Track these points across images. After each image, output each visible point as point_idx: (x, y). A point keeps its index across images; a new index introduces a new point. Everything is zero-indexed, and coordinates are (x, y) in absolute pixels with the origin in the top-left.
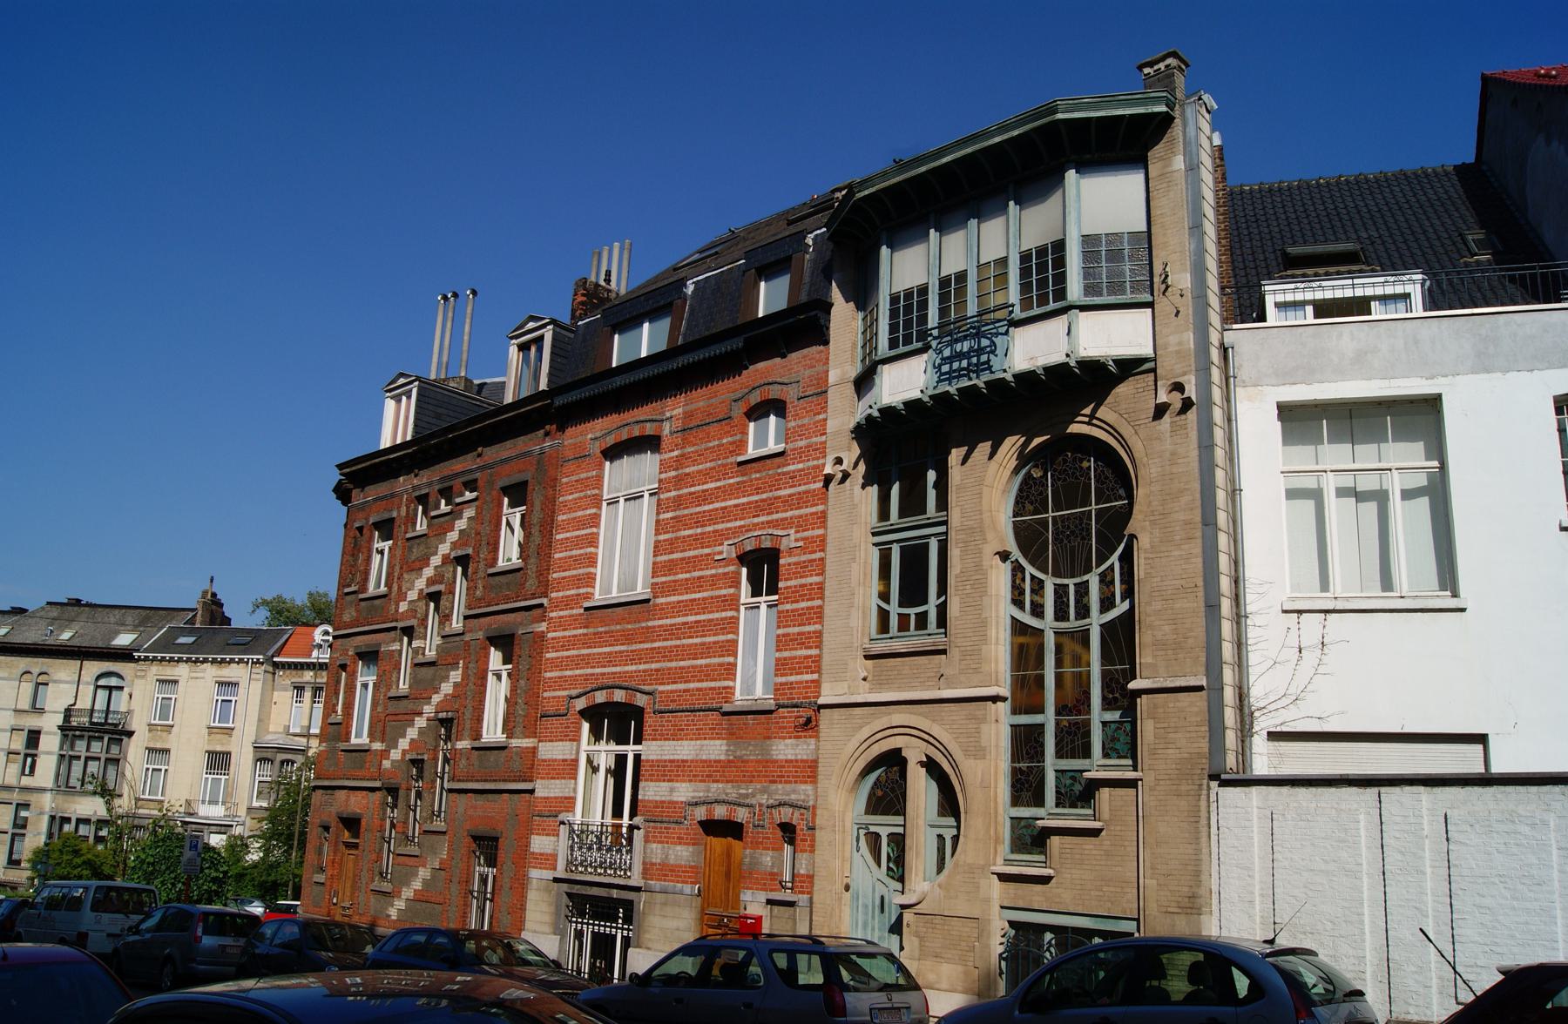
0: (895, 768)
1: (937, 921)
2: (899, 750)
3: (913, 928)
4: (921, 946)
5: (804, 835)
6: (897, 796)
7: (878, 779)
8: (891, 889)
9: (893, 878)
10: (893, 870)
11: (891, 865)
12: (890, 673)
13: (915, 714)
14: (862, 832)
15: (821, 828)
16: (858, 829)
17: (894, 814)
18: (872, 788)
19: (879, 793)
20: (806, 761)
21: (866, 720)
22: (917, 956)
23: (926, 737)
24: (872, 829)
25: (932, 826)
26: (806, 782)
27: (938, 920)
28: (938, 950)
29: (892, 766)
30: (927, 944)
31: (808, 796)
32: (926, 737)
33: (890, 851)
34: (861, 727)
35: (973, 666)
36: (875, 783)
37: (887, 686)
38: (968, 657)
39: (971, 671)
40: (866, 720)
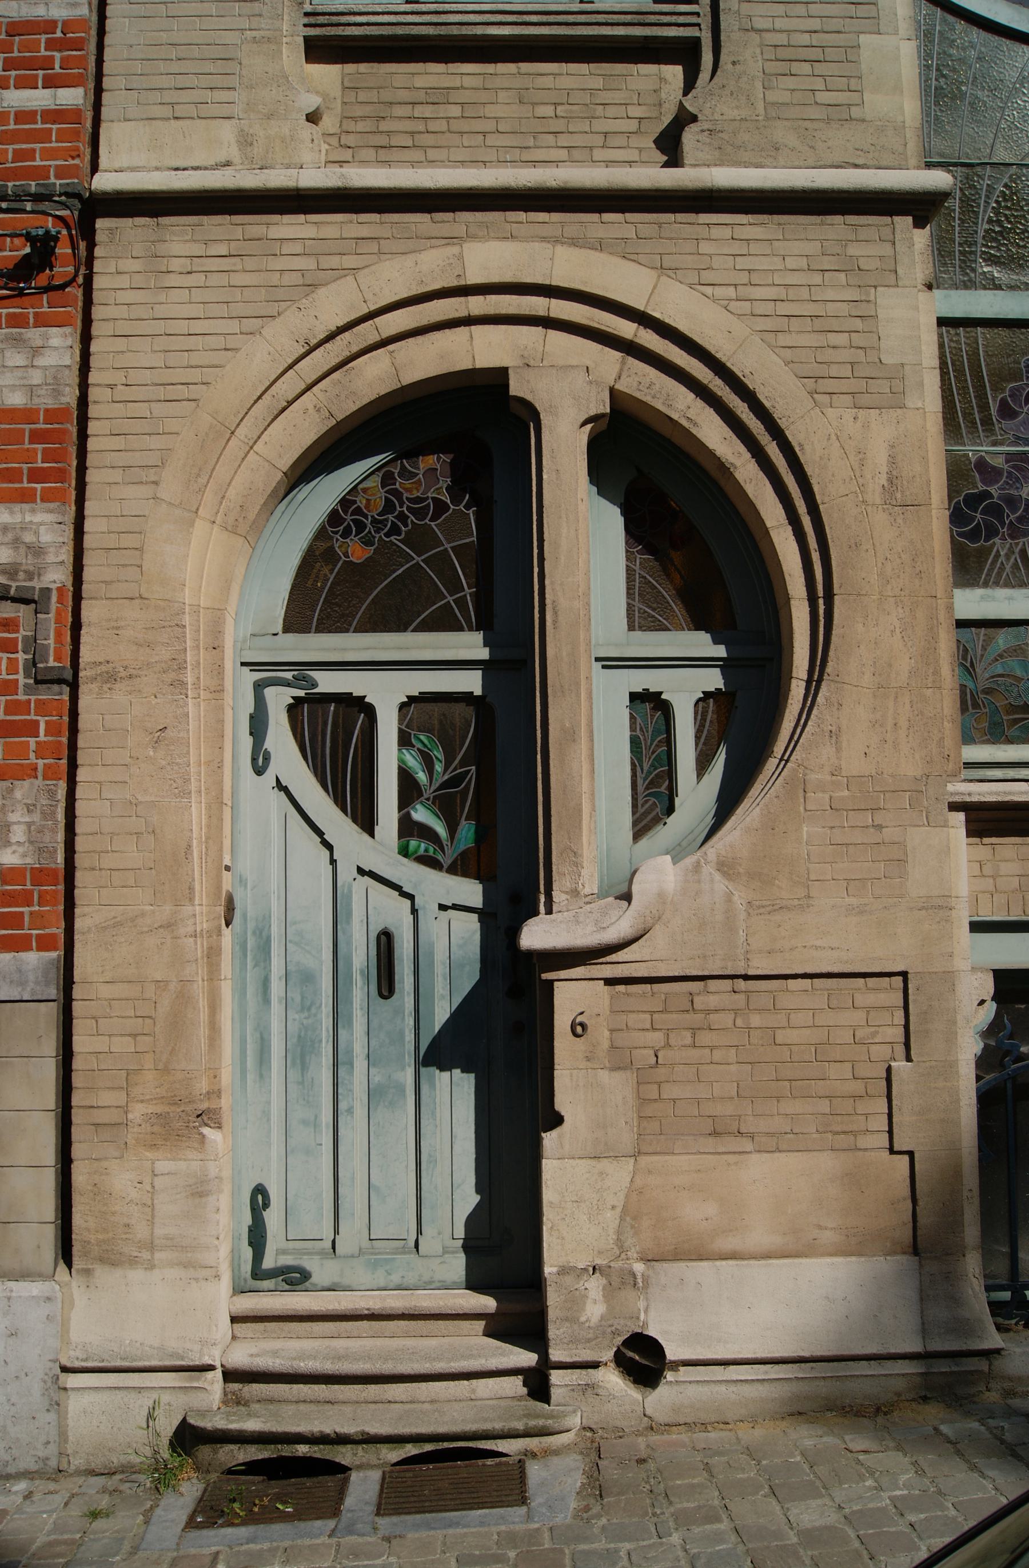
0: (430, 461)
1: (713, 1001)
2: (501, 374)
3: (600, 1034)
4: (643, 1101)
5: (22, 707)
6: (440, 564)
7: (345, 502)
8: (427, 904)
9: (428, 861)
10: (425, 832)
11: (421, 814)
12: (427, 111)
13: (574, 242)
14: (278, 699)
15: (111, 678)
16: (259, 687)
17: (426, 627)
18: (321, 534)
19: (357, 551)
20: (27, 415)
21: (334, 261)
22: (627, 1139)
23: (626, 329)
24: (328, 683)
25: (609, 663)
26: (25, 497)
27: (717, 995)
28: (728, 1109)
29: (412, 453)
30: (671, 1091)
31: (37, 551)
32: (626, 329)
33: (412, 761)
34: (313, 286)
35: (824, 97)
36: (334, 518)
37: (417, 155)
38: (806, 68)
39: (814, 113)
40: (334, 261)
